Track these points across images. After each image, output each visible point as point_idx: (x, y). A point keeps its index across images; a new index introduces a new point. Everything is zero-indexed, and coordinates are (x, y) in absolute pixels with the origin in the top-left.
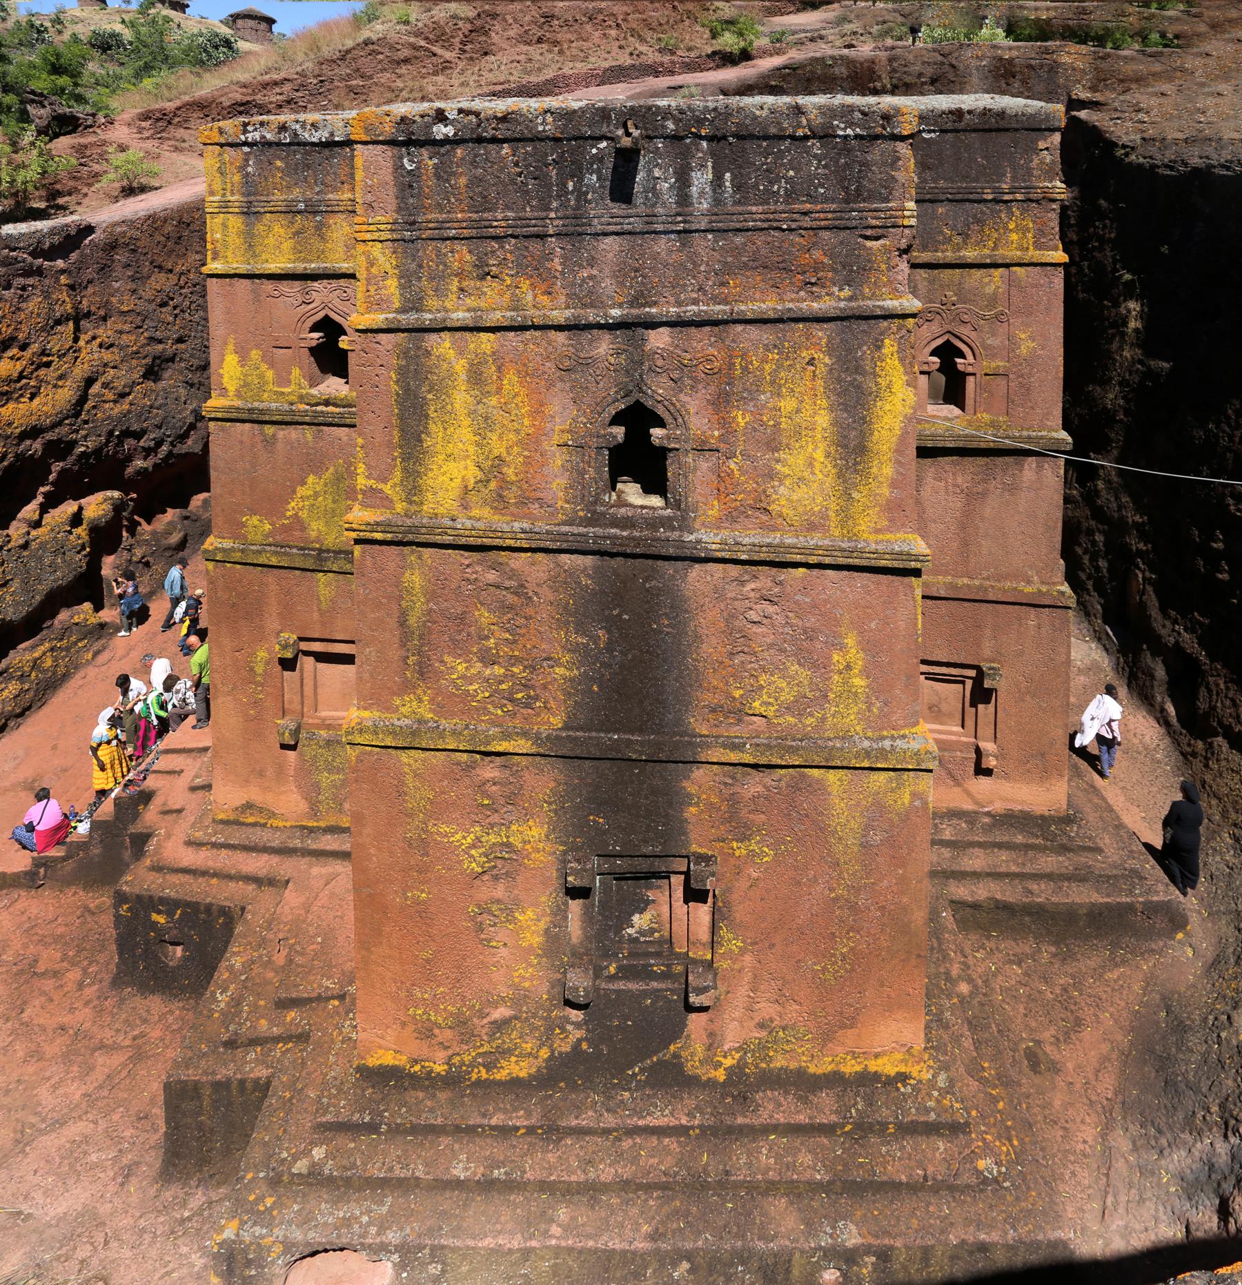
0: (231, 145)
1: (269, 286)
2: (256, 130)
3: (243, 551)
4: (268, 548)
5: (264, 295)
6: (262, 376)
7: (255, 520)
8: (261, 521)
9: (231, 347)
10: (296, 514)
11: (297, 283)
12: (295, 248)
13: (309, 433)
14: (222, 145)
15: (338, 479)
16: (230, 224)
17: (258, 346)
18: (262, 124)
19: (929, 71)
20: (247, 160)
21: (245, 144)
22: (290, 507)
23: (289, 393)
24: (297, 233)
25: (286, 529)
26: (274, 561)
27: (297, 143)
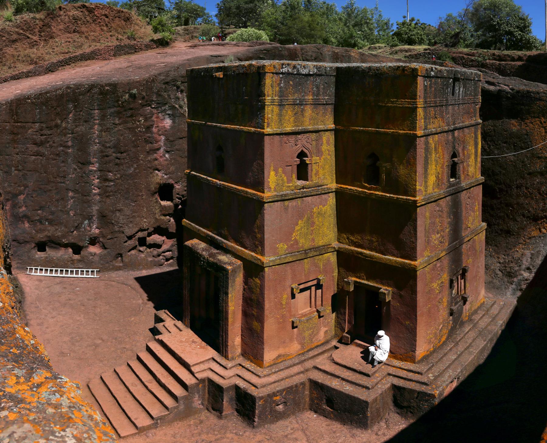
0: (277, 73)
1: (285, 138)
2: (286, 67)
3: (280, 259)
4: (288, 255)
6: (282, 180)
7: (281, 245)
8: (283, 245)
10: (295, 239)
11: (294, 136)
12: (294, 121)
13: (299, 201)
14: (273, 73)
15: (308, 219)
16: (274, 110)
17: (281, 167)
18: (288, 64)
19: (314, 55)
20: (281, 81)
21: (282, 73)
22: (293, 236)
23: (292, 186)
24: (296, 114)
25: (292, 245)
26: (291, 260)
27: (299, 74)
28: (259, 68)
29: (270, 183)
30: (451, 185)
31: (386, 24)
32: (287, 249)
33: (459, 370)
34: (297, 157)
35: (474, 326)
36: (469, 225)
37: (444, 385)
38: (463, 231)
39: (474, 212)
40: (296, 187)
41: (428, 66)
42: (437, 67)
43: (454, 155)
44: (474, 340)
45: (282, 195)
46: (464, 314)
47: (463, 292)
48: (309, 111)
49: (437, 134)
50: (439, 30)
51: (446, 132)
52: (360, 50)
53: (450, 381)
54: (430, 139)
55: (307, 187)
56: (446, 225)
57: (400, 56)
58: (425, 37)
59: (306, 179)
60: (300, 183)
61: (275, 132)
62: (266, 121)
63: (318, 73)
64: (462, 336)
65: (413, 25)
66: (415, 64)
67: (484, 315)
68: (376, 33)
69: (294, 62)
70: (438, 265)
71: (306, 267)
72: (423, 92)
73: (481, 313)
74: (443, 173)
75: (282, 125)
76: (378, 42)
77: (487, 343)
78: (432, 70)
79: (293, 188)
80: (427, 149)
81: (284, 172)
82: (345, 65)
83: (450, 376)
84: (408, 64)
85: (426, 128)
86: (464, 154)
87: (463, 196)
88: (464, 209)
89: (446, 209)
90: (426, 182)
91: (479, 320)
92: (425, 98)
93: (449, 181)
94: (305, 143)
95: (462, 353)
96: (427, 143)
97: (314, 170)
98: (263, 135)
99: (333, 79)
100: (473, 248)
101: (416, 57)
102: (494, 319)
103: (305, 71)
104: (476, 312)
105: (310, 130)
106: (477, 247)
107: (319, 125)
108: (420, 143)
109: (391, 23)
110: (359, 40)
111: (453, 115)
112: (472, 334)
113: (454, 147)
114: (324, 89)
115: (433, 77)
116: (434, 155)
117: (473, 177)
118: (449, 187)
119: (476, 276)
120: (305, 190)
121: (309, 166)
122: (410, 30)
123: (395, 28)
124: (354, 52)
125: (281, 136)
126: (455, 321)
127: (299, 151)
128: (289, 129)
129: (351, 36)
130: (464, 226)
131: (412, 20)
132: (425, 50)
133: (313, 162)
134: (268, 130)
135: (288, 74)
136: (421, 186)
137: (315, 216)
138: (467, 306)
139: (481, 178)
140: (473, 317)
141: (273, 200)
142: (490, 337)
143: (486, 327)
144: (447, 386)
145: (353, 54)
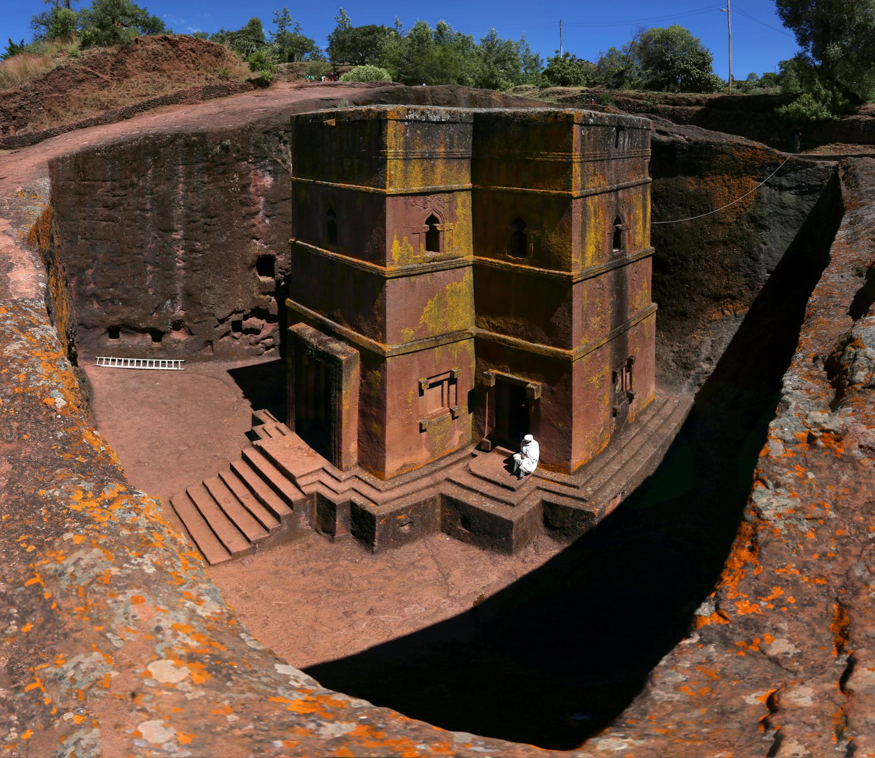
0: (401, 121)
1: (411, 200)
3: (405, 347)
6: (408, 251)
7: (407, 330)
9: (395, 236)
13: (428, 277)
15: (440, 299)
18: (415, 110)
21: (408, 120)
24: (424, 170)
25: (420, 331)
26: (418, 348)
28: (379, 114)
30: (614, 257)
31: (535, 60)
32: (414, 335)
33: (624, 483)
34: (427, 223)
35: (641, 430)
36: (636, 306)
37: (606, 501)
38: (629, 313)
39: (642, 289)
40: (425, 260)
41: (585, 112)
42: (597, 112)
43: (618, 221)
44: (642, 446)
45: (407, 270)
46: (630, 415)
47: (628, 388)
48: (440, 166)
49: (597, 194)
50: (599, 67)
51: (607, 192)
52: (503, 93)
53: (612, 496)
54: (589, 201)
56: (608, 305)
57: (552, 99)
58: (582, 77)
59: (437, 250)
60: (430, 254)
62: (388, 179)
63: (452, 120)
64: (627, 441)
65: (567, 61)
66: (570, 109)
67: (654, 416)
68: (522, 71)
69: (422, 107)
70: (599, 355)
71: (437, 356)
72: (579, 143)
73: (650, 413)
74: (604, 242)
75: (408, 183)
76: (525, 83)
77: (658, 451)
78: (591, 116)
79: (421, 260)
80: (585, 213)
81: (410, 241)
82: (484, 110)
83: (612, 491)
84: (561, 110)
85: (583, 188)
86: (629, 219)
87: (629, 269)
88: (629, 286)
89: (607, 287)
90: (583, 253)
91: (649, 421)
92: (582, 150)
93: (611, 252)
94: (436, 206)
95: (627, 462)
96: (584, 206)
98: (384, 196)
99: (470, 128)
100: (641, 334)
101: (571, 101)
102: (666, 420)
103: (435, 118)
104: (644, 412)
106: (646, 333)
108: (576, 205)
109: (540, 59)
110: (502, 80)
111: (616, 171)
112: (640, 440)
113: (617, 211)
114: (458, 139)
115: (592, 125)
116: (593, 220)
117: (641, 247)
118: (612, 259)
119: (645, 368)
121: (441, 233)
122: (564, 68)
123: (545, 65)
124: (495, 95)
126: (619, 423)
127: (429, 215)
128: (416, 188)
129: (492, 76)
130: (630, 307)
131: (567, 55)
132: (583, 91)
134: (390, 190)
135: (415, 121)
136: (577, 258)
137: (448, 295)
138: (633, 405)
139: (650, 249)
140: (641, 418)
141: (397, 275)
142: (661, 442)
143: (657, 431)
144: (609, 502)
145: (494, 97)
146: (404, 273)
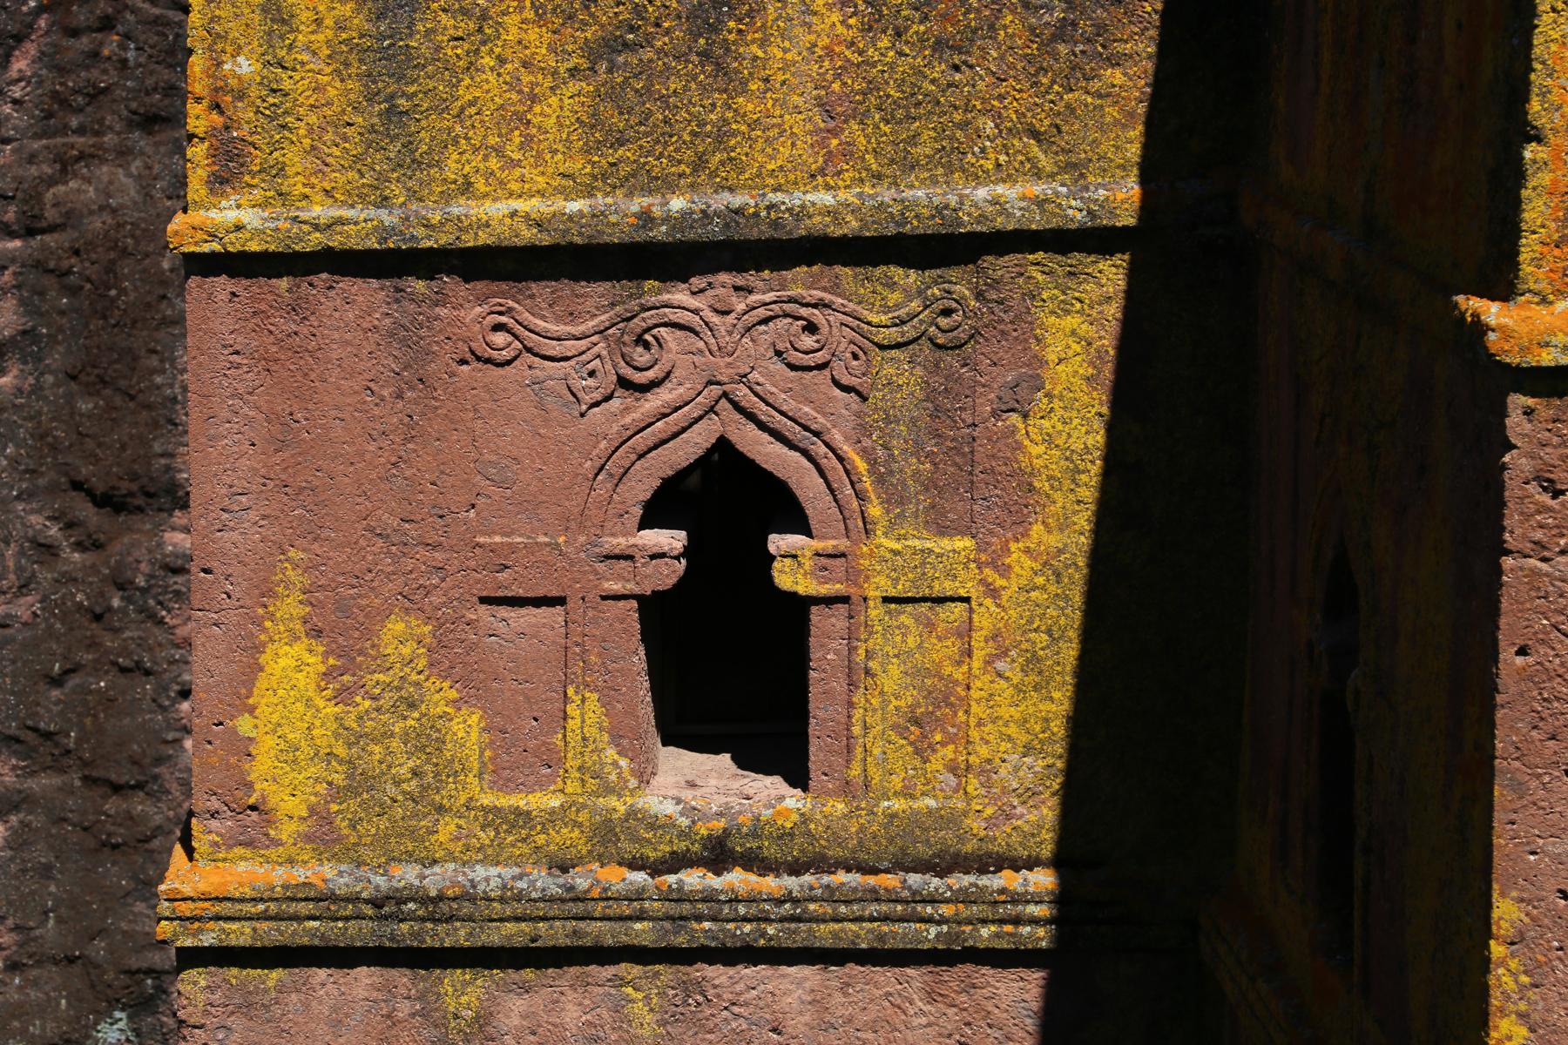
5: (447, 354)
6: (427, 741)
9: (290, 607)
11: (598, 291)
12: (594, 122)
17: (411, 601)
23: (553, 818)
24: (610, 47)
29: (262, 766)
45: (385, 904)
55: (770, 850)
61: (315, 241)
62: (198, 118)
75: (413, 163)
79: (568, 837)
94: (772, 377)
97: (891, 677)
105: (818, 224)
107: (978, 178)
120: (736, 879)
121: (825, 626)
125: (419, 286)
133: (881, 584)
141: (272, 934)
146: (361, 933)
